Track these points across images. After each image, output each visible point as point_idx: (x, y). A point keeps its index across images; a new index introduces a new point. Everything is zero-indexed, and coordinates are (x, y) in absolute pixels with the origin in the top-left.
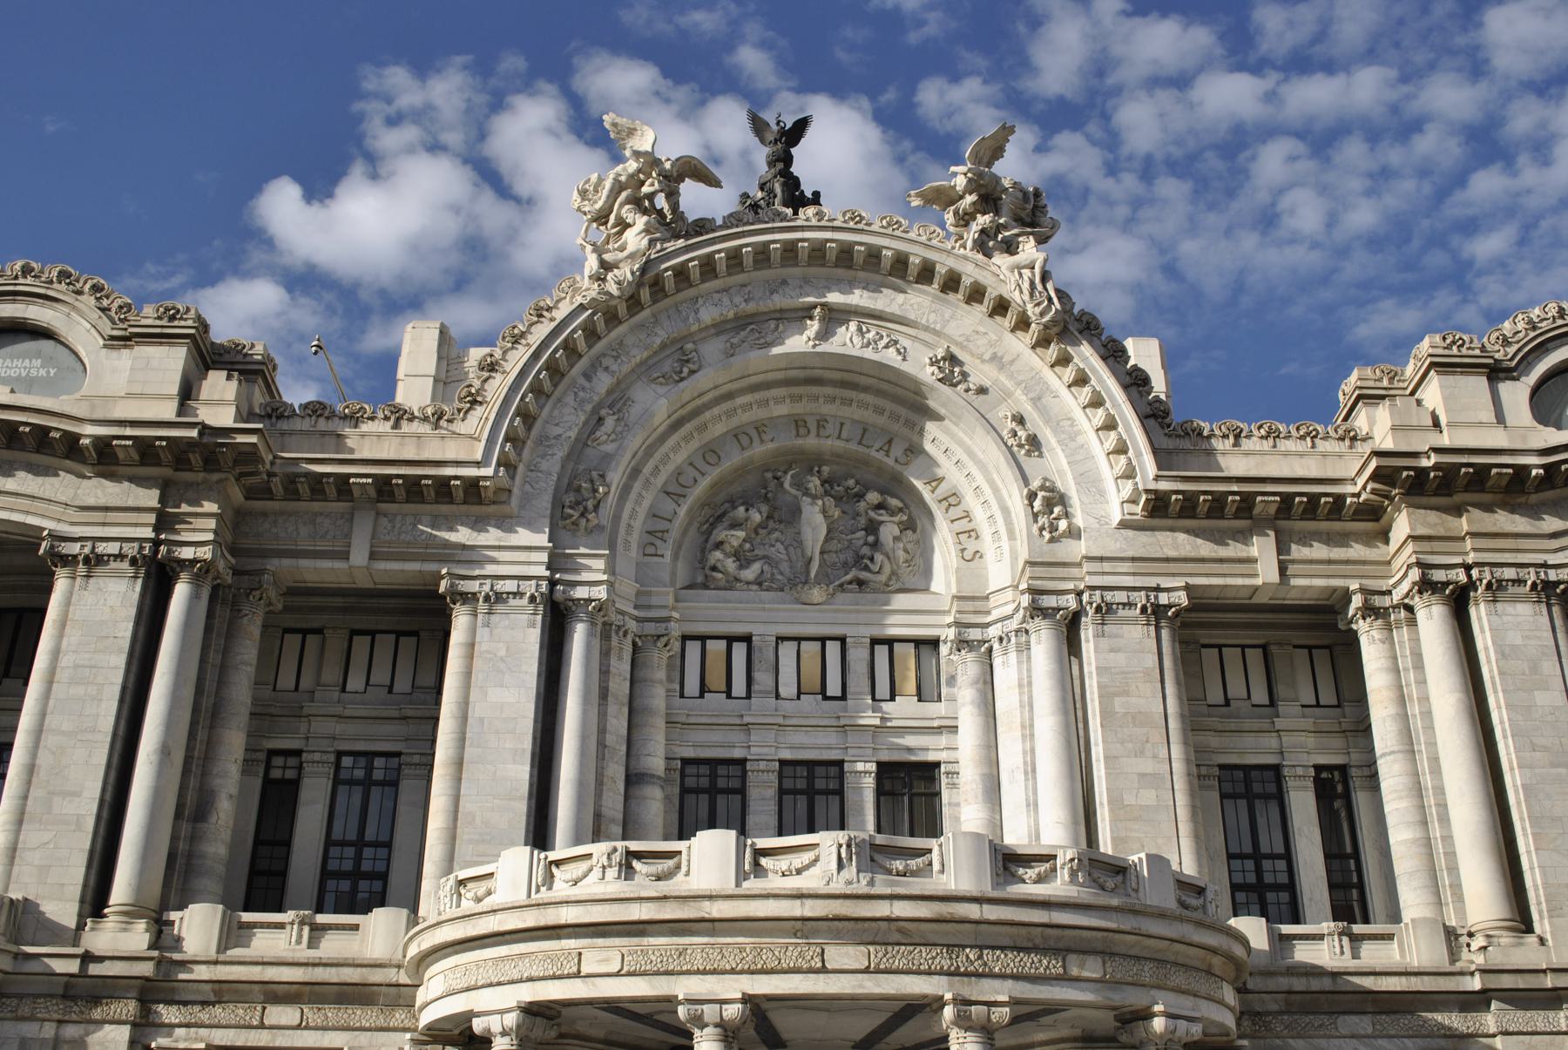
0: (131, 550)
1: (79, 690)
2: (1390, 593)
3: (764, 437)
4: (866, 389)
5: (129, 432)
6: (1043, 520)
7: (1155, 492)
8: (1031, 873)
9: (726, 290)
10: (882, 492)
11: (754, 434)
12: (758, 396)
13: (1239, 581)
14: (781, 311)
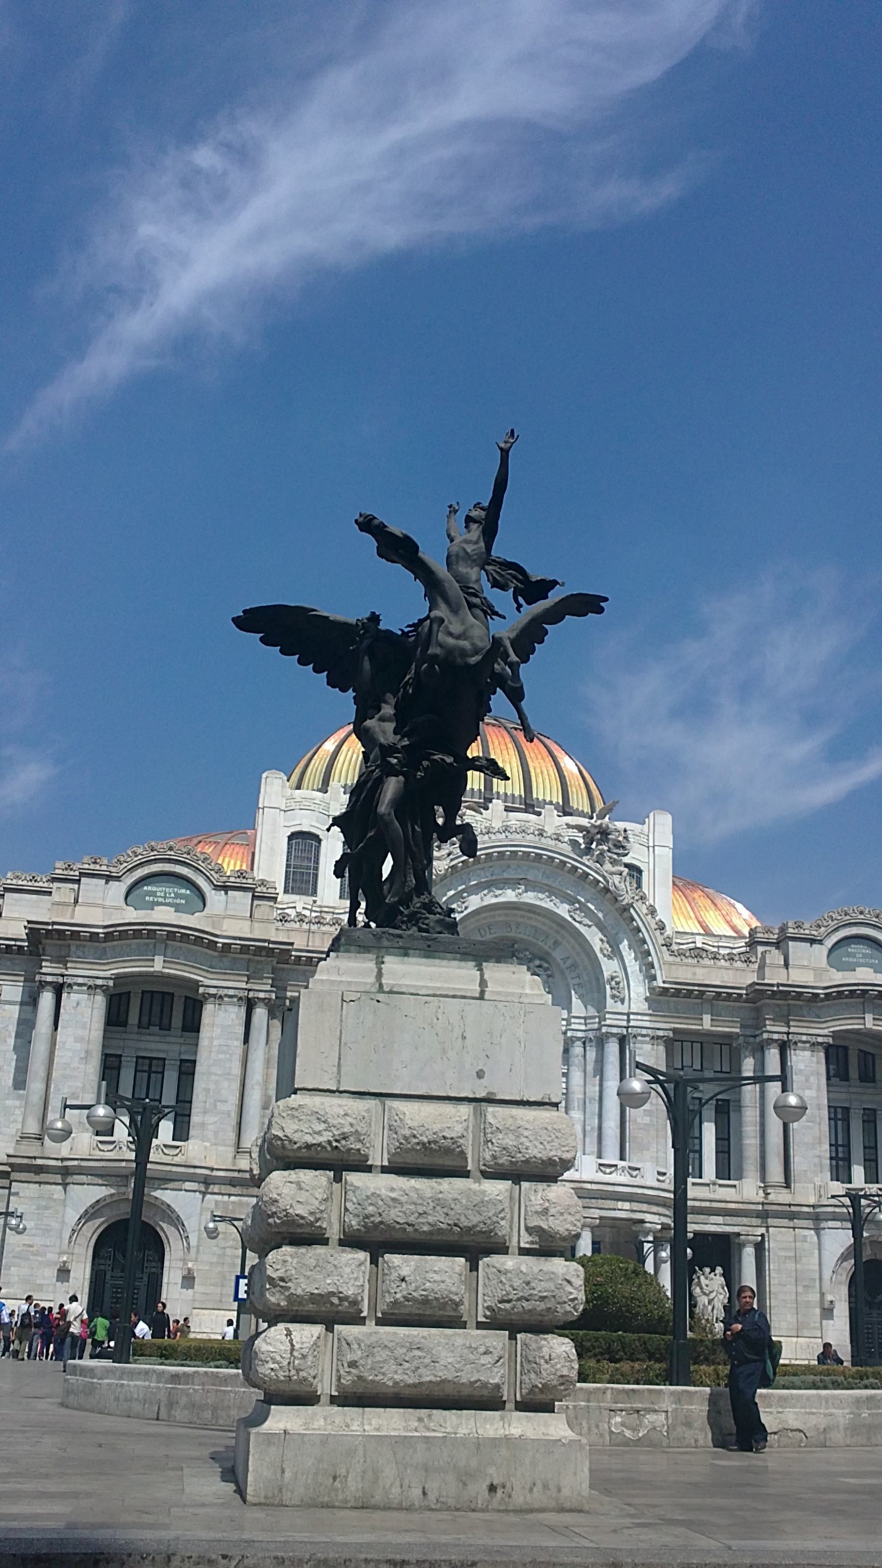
0: (242, 994)
1: (222, 1056)
2: (755, 1036)
3: (492, 931)
4: (539, 914)
5: (238, 942)
6: (615, 992)
7: (663, 988)
8: (608, 1170)
9: (483, 869)
10: (541, 959)
11: (487, 930)
12: (492, 913)
13: (694, 1027)
14: (507, 879)
